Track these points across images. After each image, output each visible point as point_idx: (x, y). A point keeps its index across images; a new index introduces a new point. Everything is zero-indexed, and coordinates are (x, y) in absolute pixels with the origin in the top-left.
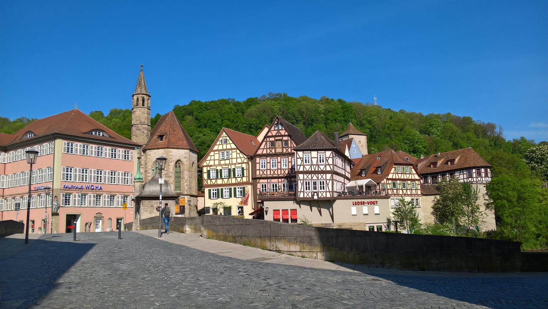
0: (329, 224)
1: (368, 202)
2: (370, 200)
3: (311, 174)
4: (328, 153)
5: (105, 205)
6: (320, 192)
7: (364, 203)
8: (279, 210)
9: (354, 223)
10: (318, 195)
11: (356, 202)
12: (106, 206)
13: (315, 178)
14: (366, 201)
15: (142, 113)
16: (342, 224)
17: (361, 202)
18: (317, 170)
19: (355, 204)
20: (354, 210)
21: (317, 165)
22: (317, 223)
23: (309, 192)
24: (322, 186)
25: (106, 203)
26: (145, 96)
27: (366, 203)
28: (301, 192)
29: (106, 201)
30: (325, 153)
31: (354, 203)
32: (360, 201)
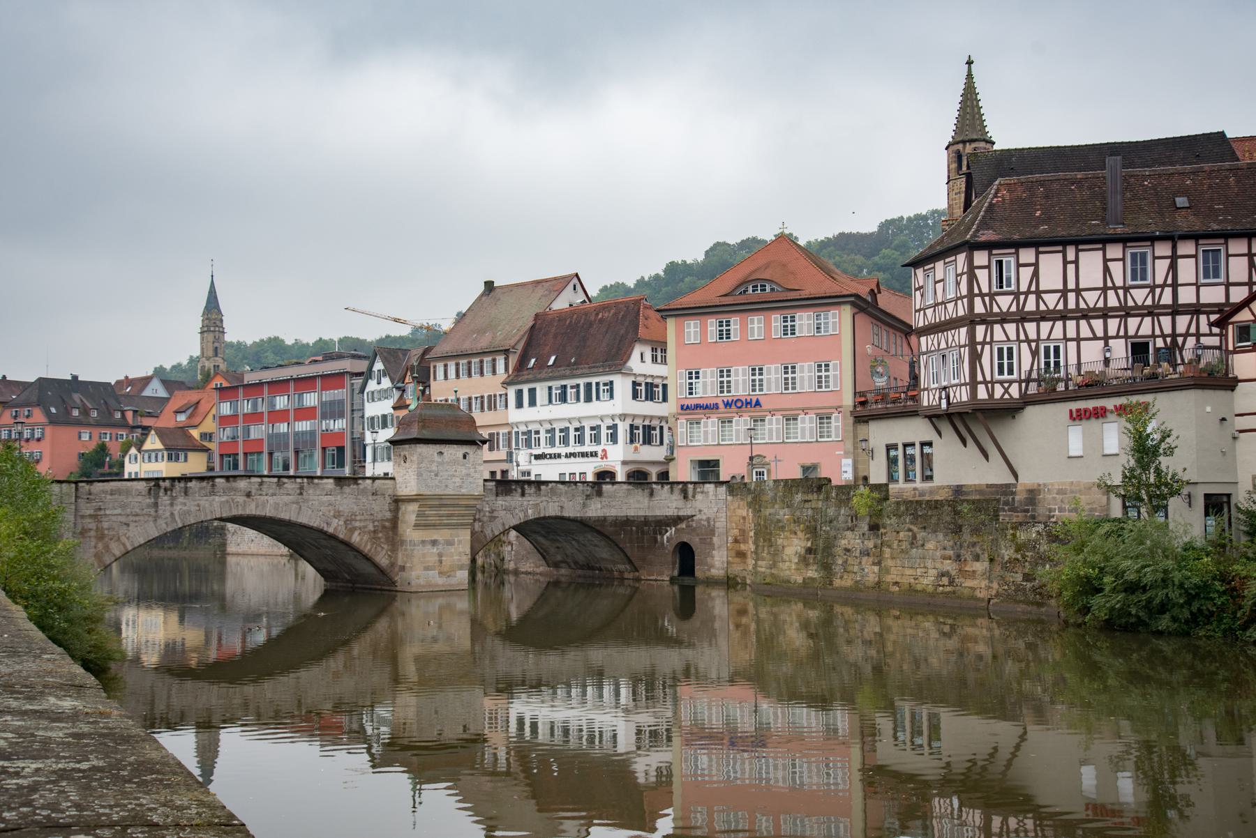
0: (1006, 485)
1: (1115, 406)
2: (1122, 401)
3: (937, 332)
4: (961, 258)
5: (772, 439)
6: (952, 386)
7: (1100, 413)
8: (896, 445)
9: (1072, 482)
10: (948, 397)
11: (1078, 410)
12: (774, 441)
13: (943, 345)
14: (1110, 403)
15: (956, 194)
16: (1039, 485)
17: (1095, 409)
18: (943, 319)
19: (1078, 416)
20: (1076, 440)
21: (958, 299)
22: (977, 482)
23: (936, 389)
24: (1005, 361)
25: (774, 434)
26: (960, 146)
27: (1112, 412)
28: (925, 389)
29: (774, 429)
30: (1015, 256)
31: (1074, 416)
32: (1090, 404)
